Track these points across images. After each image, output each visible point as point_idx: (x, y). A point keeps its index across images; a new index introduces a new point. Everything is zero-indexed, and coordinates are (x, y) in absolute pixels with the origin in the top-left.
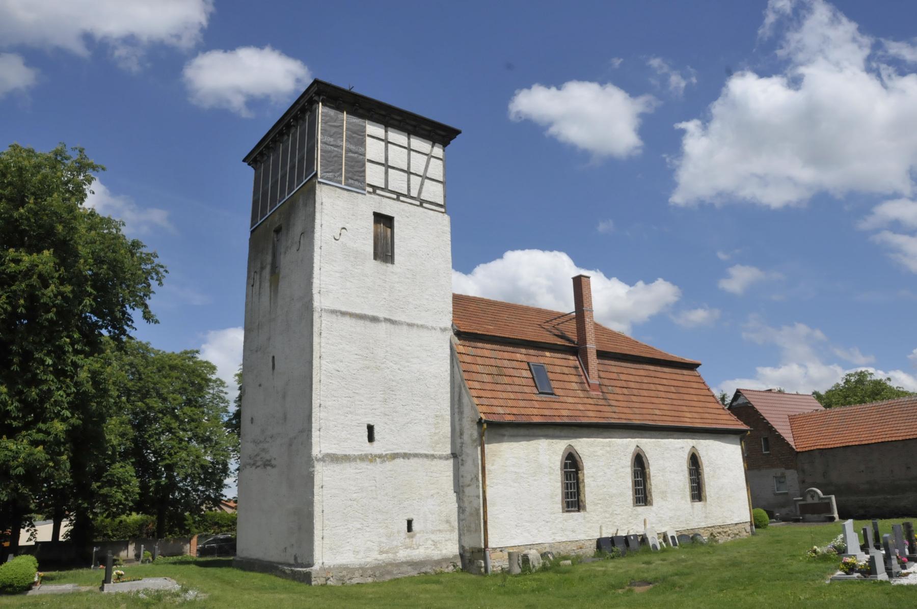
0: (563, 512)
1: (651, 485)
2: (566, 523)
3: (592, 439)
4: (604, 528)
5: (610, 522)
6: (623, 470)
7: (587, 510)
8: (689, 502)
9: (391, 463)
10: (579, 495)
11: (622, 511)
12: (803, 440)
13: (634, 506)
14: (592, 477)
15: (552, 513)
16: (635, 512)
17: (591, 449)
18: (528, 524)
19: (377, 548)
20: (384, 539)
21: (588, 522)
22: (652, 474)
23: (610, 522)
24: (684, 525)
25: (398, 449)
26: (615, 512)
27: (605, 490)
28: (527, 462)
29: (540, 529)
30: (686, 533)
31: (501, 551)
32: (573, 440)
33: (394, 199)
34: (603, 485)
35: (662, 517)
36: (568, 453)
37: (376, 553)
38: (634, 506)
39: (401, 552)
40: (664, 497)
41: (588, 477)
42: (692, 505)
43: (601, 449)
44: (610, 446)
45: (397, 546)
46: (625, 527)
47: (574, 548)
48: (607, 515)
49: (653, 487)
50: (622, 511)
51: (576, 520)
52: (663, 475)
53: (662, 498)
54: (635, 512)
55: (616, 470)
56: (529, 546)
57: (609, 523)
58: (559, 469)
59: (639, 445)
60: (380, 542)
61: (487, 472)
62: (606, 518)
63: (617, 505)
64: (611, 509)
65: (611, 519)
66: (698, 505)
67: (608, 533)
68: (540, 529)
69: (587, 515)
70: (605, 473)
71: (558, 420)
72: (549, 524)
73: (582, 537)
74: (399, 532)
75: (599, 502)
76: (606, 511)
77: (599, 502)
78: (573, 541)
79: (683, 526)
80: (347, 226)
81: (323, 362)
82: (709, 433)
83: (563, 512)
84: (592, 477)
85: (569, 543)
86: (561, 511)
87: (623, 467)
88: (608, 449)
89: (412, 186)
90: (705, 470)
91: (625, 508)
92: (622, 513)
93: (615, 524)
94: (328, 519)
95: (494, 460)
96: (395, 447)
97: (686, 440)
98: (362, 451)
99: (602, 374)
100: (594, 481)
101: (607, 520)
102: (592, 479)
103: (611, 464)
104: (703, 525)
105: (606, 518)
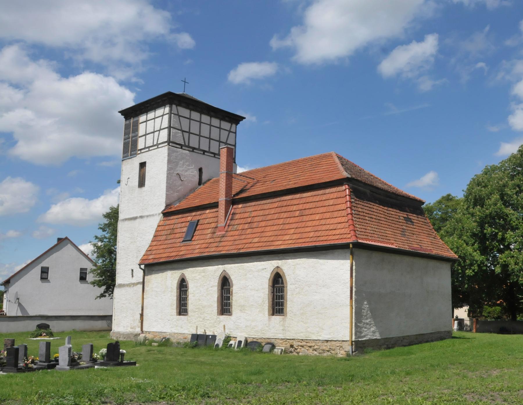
0: (177, 315)
1: (232, 300)
2: (178, 322)
3: (194, 269)
4: (198, 328)
5: (203, 324)
9: (136, 287)
10: (273, 304)
11: (210, 318)
12: (434, 246)
13: (218, 315)
14: (193, 293)
15: (171, 315)
16: (218, 320)
17: (193, 275)
18: (160, 320)
19: (130, 326)
20: (132, 322)
21: (190, 323)
22: (234, 292)
23: (203, 324)
24: (259, 334)
26: (206, 318)
27: (200, 302)
28: (162, 285)
29: (165, 324)
30: (259, 341)
31: (149, 333)
32: (184, 270)
33: (148, 151)
34: (199, 299)
35: (238, 325)
36: (181, 278)
38: (218, 315)
39: (137, 329)
40: (243, 309)
42: (269, 318)
43: (199, 275)
44: (204, 272)
45: (136, 326)
46: (212, 329)
47: (181, 338)
48: (201, 320)
49: (233, 302)
51: (183, 321)
53: (241, 310)
54: (218, 320)
55: (208, 289)
56: (315, 341)
57: (202, 325)
58: (176, 289)
59: (225, 270)
60: (131, 324)
61: (145, 291)
62: (200, 321)
63: (207, 314)
64: (203, 315)
66: (277, 318)
67: (200, 332)
68: (165, 324)
69: (189, 318)
70: (201, 291)
71: (161, 260)
72: (169, 321)
73: (186, 332)
74: (137, 320)
75: (197, 310)
76: (200, 317)
77: (197, 310)
78: (181, 334)
79: (258, 334)
80: (130, 176)
82: (305, 251)
83: (177, 315)
84: (193, 293)
85: (179, 335)
87: (212, 287)
88: (203, 274)
89: (155, 140)
90: (288, 288)
91: (212, 316)
92: (210, 319)
93: (206, 326)
94: (116, 312)
95: (148, 285)
97: (270, 262)
99: (215, 220)
100: (194, 296)
101: (201, 323)
102: (193, 295)
103: (204, 285)
104: (281, 336)
105: (200, 321)
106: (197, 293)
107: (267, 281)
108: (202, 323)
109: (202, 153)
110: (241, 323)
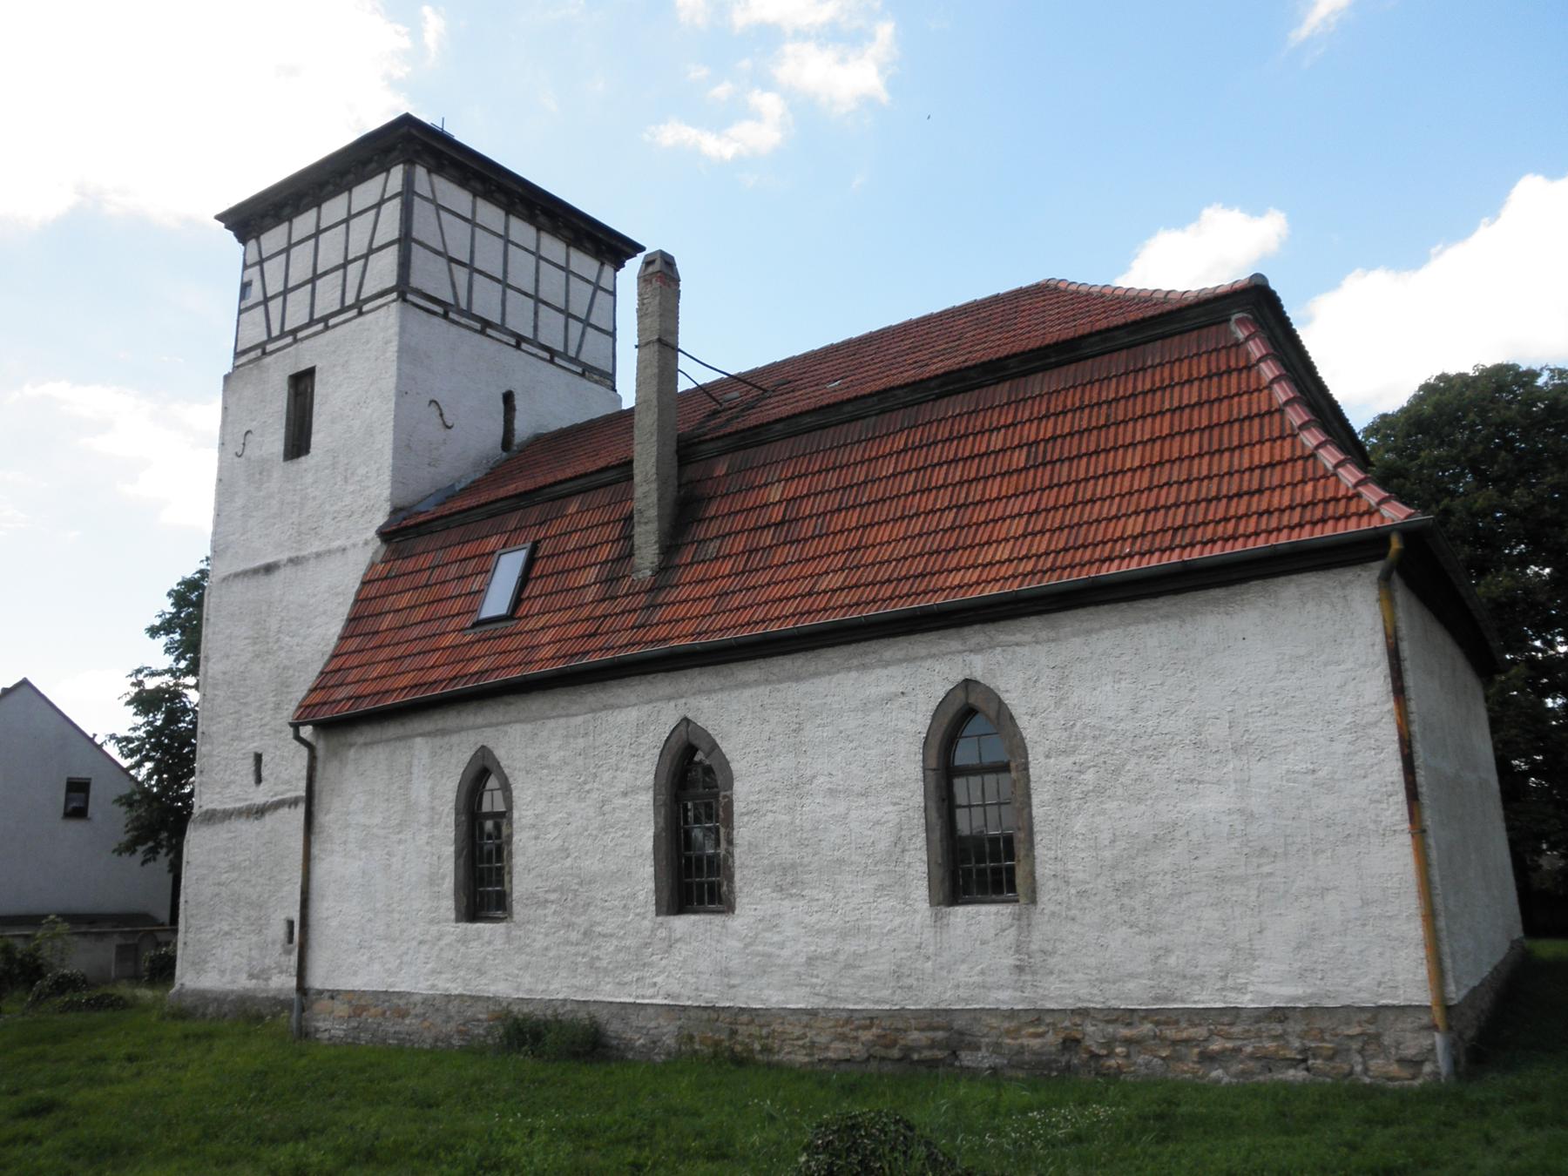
0: (458, 920)
2: (463, 949)
6: (626, 801)
7: (516, 917)
8: (923, 906)
13: (658, 913)
15: (432, 922)
18: (383, 944)
19: (247, 968)
21: (520, 950)
22: (738, 807)
23: (584, 955)
25: (289, 791)
26: (599, 929)
27: (568, 862)
31: (332, 998)
35: (770, 956)
37: (245, 976)
38: (658, 913)
40: (788, 880)
41: (742, 814)
42: (937, 918)
45: (269, 968)
47: (481, 1016)
48: (574, 936)
49: (737, 852)
50: (621, 927)
51: (489, 943)
52: (790, 809)
54: (662, 933)
59: (690, 716)
61: (316, 829)
62: (568, 942)
65: (582, 949)
74: (274, 943)
75: (553, 896)
79: (878, 995)
80: (252, 426)
81: (210, 664)
83: (458, 920)
86: (453, 916)
87: (625, 794)
89: (347, 289)
96: (285, 787)
98: (246, 800)
101: (573, 950)
103: (587, 787)
105: (568, 942)
106: (555, 824)
107: (917, 748)
108: (582, 949)
109: (513, 342)
110: (782, 946)
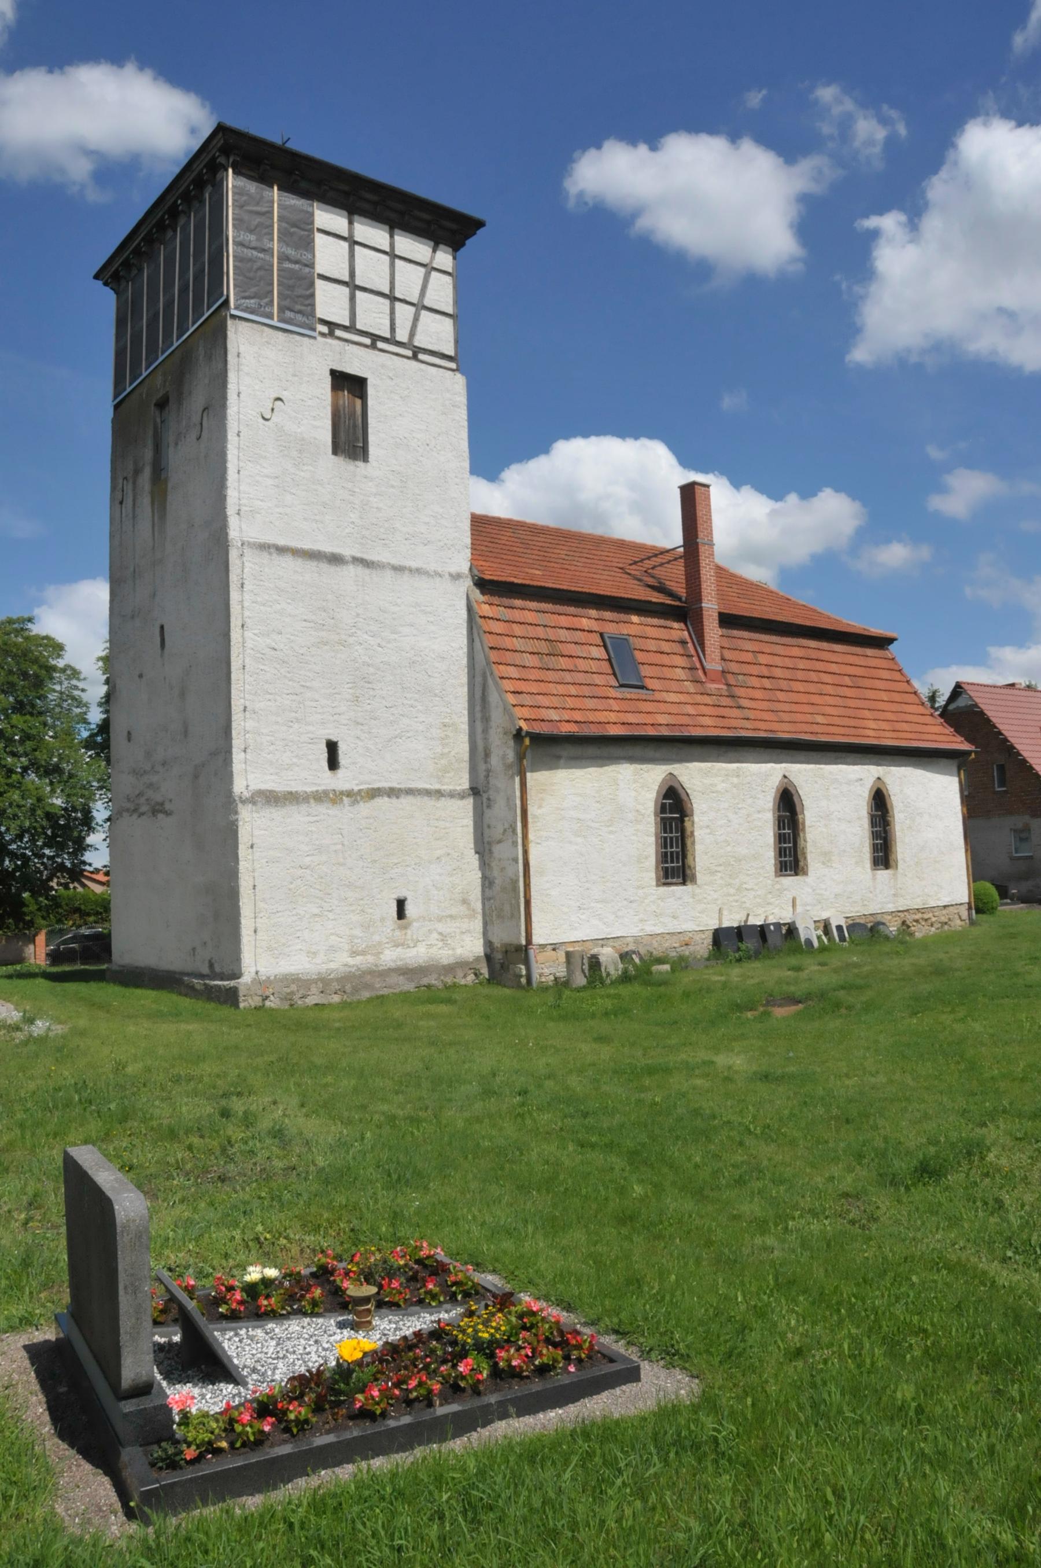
0: (658, 885)
1: (805, 841)
2: (662, 904)
3: (709, 764)
4: (725, 913)
5: (737, 901)
6: (760, 816)
7: (699, 882)
8: (869, 870)
11: (756, 884)
14: (708, 826)
15: (638, 887)
16: (777, 886)
17: (707, 781)
18: (599, 905)
19: (347, 947)
20: (358, 932)
22: (807, 823)
23: (737, 901)
25: (380, 781)
26: (745, 886)
27: (729, 849)
30: (862, 921)
31: (554, 950)
33: (366, 346)
34: (726, 841)
37: (345, 954)
39: (387, 952)
41: (701, 828)
42: (874, 875)
43: (723, 781)
44: (738, 776)
45: (380, 943)
46: (760, 911)
48: (732, 891)
49: (808, 845)
50: (756, 884)
51: (680, 898)
52: (826, 826)
53: (823, 863)
54: (777, 886)
55: (748, 816)
61: (530, 820)
62: (729, 895)
63: (748, 875)
65: (736, 898)
66: (883, 874)
67: (731, 921)
69: (698, 891)
71: (651, 732)
72: (634, 905)
73: (689, 926)
74: (382, 920)
78: (673, 934)
80: (284, 395)
81: (248, 634)
83: (658, 885)
84: (708, 826)
85: (668, 937)
86: (654, 883)
87: (759, 812)
88: (735, 780)
89: (398, 322)
92: (756, 888)
94: (264, 900)
95: (542, 799)
96: (374, 777)
97: (866, 767)
98: (319, 785)
99: (728, 655)
101: (731, 899)
102: (708, 831)
104: (891, 907)
105: (729, 895)
106: (721, 826)
107: (865, 804)
108: (736, 898)
110: (826, 890)
